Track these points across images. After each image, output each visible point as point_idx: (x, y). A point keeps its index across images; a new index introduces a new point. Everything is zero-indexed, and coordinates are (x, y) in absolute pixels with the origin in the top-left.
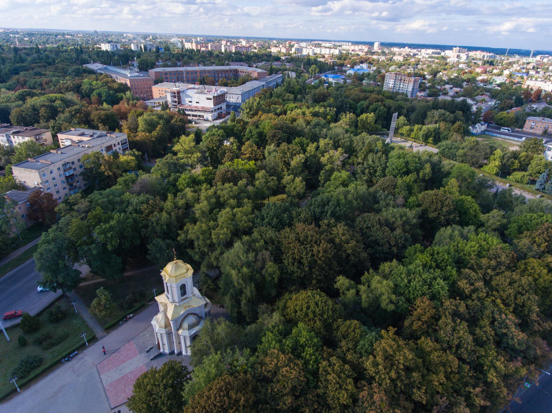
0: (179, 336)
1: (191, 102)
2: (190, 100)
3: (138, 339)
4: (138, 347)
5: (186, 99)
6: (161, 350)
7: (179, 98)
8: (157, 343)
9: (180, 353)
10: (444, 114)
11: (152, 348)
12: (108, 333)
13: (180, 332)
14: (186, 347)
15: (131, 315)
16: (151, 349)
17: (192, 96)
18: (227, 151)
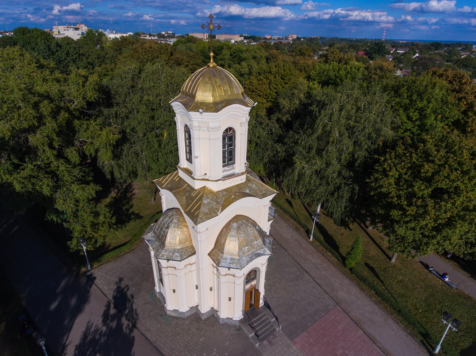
11: (252, 328)
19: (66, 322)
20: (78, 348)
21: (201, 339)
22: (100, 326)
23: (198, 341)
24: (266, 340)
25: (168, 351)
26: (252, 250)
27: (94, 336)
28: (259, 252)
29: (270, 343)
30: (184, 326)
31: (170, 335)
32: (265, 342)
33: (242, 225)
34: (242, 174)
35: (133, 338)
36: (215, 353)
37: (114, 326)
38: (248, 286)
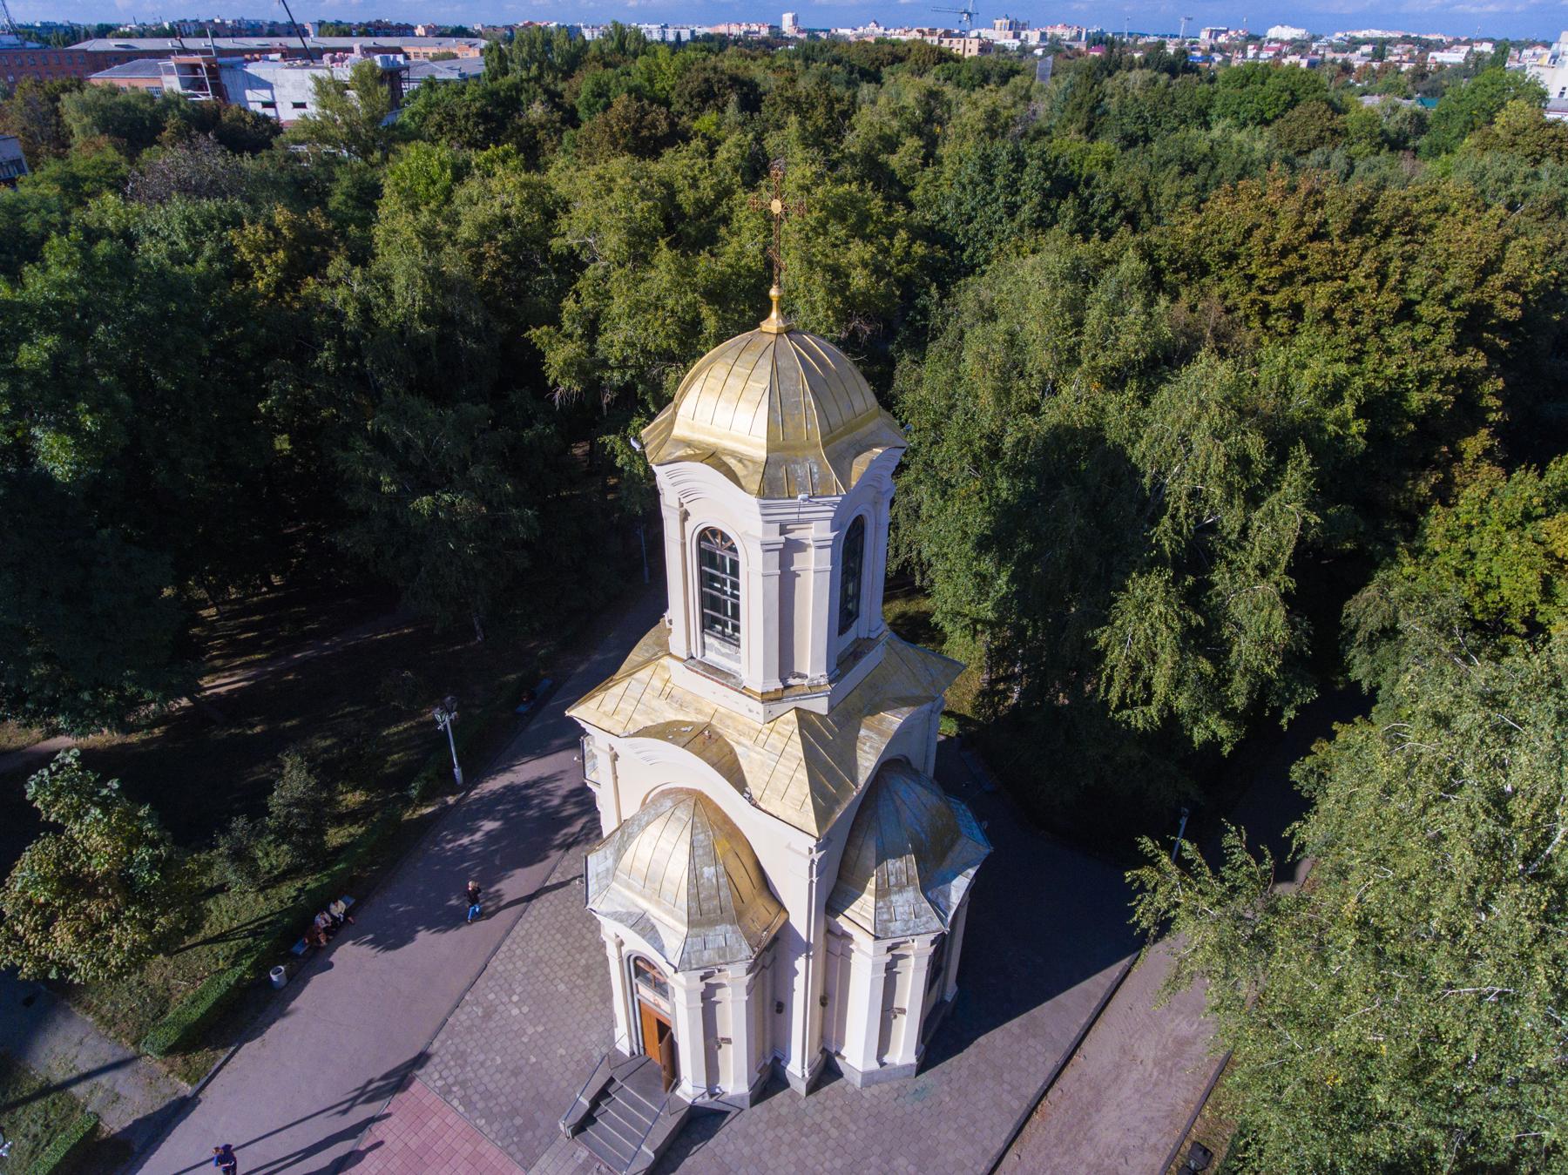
0: (835, 946)
1: (272, 105)
2: (265, 95)
3: (461, 1057)
4: (490, 1117)
5: (250, 95)
6: (690, 1088)
7: (219, 90)
8: (624, 1045)
9: (827, 1070)
10: (1154, 81)
11: (603, 1093)
12: (203, 1079)
13: (861, 911)
14: (888, 1012)
15: (339, 908)
16: (595, 1103)
17: (270, 79)
18: (541, 135)
19: (557, 742)
20: (510, 789)
21: (562, 987)
22: (562, 792)
23: (557, 981)
24: (591, 1155)
25: (523, 933)
26: (644, 904)
27: (536, 796)
28: (659, 927)
29: (585, 1167)
30: (589, 936)
31: (561, 918)
32: (583, 1153)
33: (679, 819)
34: (745, 691)
35: (547, 857)
36: (530, 1031)
37: (565, 813)
38: (646, 993)
